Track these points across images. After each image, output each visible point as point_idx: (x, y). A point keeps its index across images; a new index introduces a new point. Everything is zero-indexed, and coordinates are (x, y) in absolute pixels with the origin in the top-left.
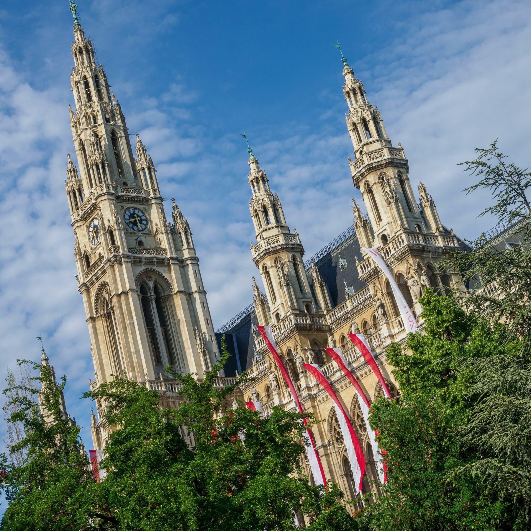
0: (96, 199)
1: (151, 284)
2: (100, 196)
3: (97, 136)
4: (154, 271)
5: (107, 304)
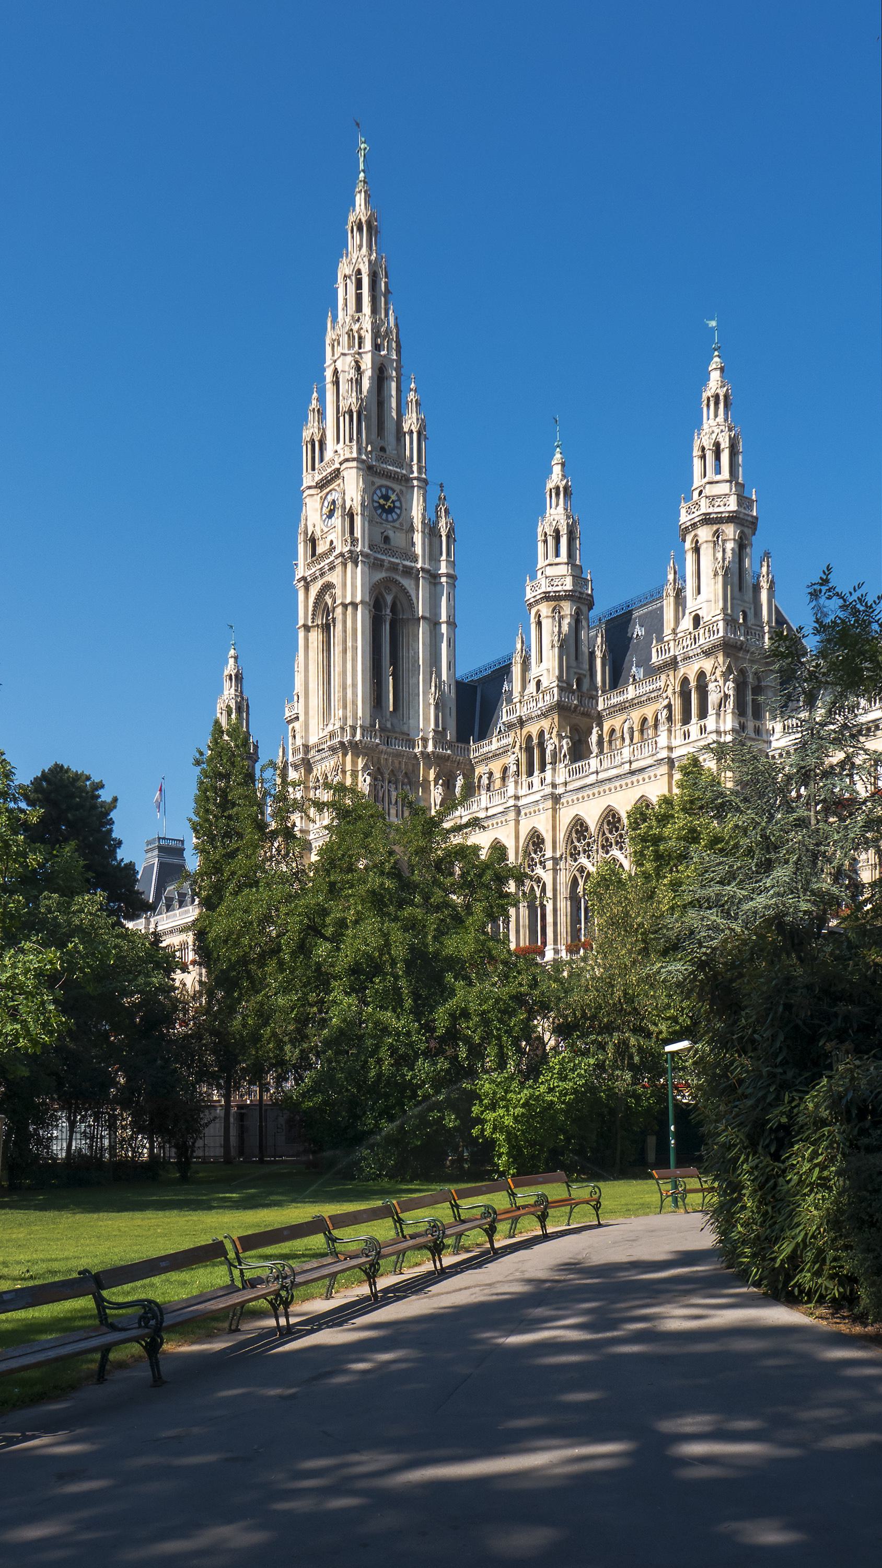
0: (341, 464)
1: (389, 599)
2: (347, 460)
3: (358, 368)
4: (396, 583)
5: (328, 611)
